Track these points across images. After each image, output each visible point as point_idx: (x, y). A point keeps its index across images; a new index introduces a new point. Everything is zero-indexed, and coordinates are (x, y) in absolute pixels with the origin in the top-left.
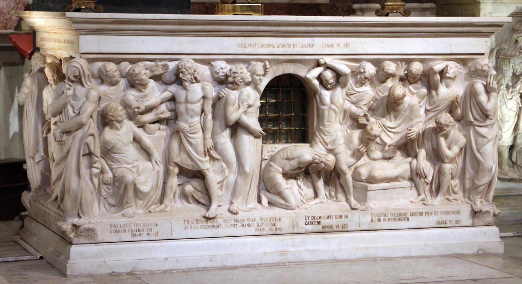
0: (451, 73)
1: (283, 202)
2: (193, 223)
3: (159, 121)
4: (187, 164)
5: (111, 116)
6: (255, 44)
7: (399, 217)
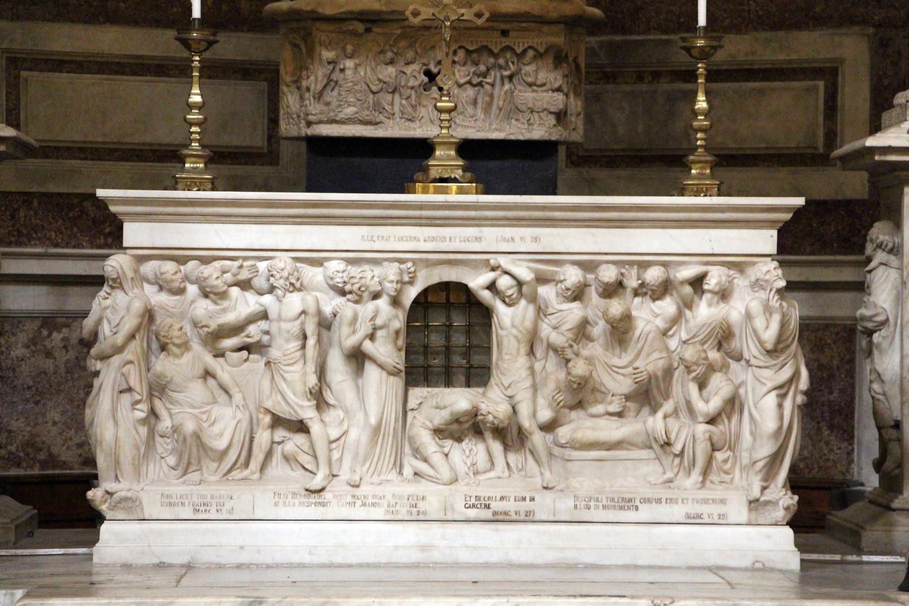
0: (711, 283)
1: (431, 472)
3: (247, 348)
4: (284, 411)
5: (164, 336)
6: (389, 237)
7: (621, 504)
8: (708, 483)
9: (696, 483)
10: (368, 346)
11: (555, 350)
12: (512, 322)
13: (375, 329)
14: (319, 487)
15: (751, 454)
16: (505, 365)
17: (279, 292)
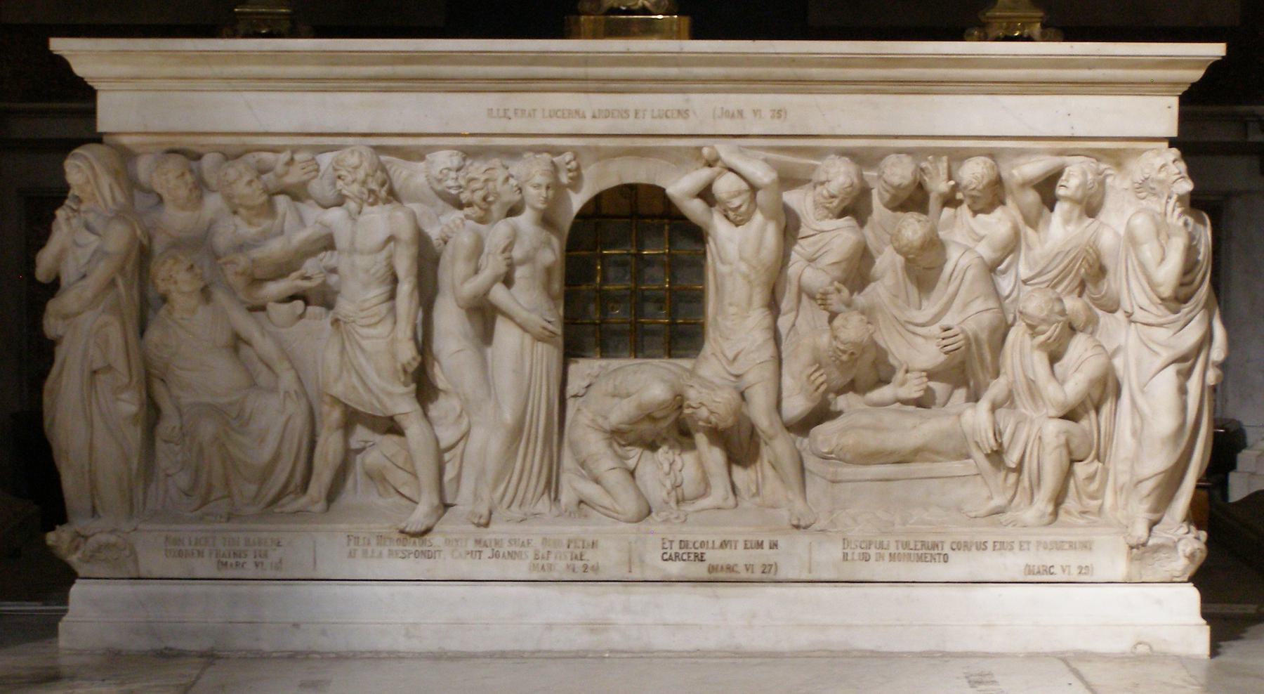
0: (1070, 185)
2: (369, 544)
4: (364, 403)
6: (534, 110)
7: (920, 552)
8: (1062, 516)
9: (1042, 516)
10: (499, 294)
11: (812, 297)
12: (740, 252)
13: (511, 266)
14: (421, 528)
15: (1132, 467)
16: (729, 324)
17: (352, 205)
